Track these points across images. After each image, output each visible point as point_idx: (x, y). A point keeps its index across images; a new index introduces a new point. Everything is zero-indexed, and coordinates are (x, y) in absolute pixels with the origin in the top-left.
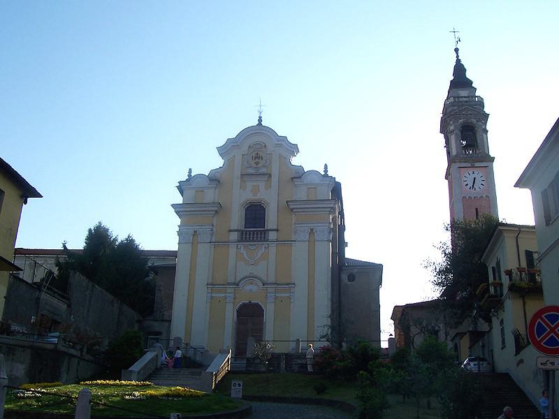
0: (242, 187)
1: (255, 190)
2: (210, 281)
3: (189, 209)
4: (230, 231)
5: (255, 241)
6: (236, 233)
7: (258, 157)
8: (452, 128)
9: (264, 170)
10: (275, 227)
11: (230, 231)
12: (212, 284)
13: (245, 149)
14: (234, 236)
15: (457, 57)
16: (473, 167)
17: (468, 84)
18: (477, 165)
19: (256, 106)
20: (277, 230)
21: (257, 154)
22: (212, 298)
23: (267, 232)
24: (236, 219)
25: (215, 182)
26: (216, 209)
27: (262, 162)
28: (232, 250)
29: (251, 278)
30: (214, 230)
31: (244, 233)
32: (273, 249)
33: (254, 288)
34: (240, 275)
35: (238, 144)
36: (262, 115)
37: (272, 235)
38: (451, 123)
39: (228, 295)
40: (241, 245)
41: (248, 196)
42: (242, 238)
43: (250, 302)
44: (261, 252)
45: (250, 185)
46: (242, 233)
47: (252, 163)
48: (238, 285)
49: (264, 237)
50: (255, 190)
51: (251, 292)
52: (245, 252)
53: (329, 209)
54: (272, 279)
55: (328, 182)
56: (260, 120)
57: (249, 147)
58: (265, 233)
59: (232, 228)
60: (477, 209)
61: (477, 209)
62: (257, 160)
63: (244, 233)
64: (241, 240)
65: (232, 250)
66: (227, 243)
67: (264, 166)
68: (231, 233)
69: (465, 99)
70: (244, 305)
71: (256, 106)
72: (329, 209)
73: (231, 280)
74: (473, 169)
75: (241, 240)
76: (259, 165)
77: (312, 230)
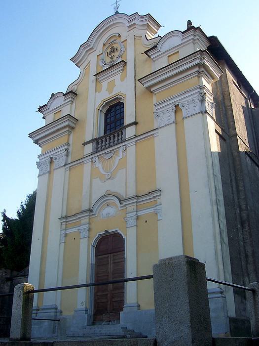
1: (111, 86)
2: (64, 215)
4: (84, 144)
10: (133, 120)
12: (66, 217)
13: (100, 49)
22: (66, 235)
27: (116, 54)
32: (131, 149)
33: (111, 210)
39: (81, 227)
45: (105, 84)
46: (98, 143)
51: (109, 218)
53: (197, 69)
54: (131, 192)
55: (192, 37)
57: (104, 45)
64: (96, 150)
65: (87, 167)
66: (79, 161)
73: (86, 206)
75: (96, 150)
76: (115, 59)
77: (177, 106)
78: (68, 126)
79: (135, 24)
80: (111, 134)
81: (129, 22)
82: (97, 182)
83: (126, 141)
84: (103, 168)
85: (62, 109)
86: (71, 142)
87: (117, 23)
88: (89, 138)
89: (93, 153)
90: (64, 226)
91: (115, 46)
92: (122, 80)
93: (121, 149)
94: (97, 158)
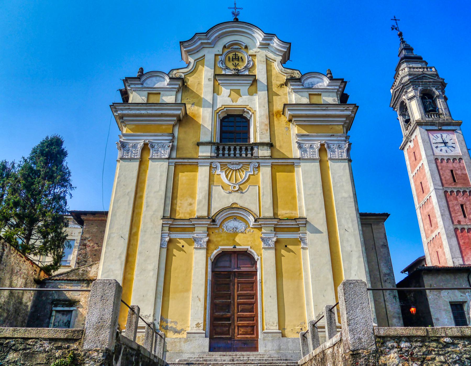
3: (138, 112)
4: (199, 144)
5: (237, 158)
6: (209, 148)
8: (411, 95)
9: (247, 73)
10: (267, 140)
13: (219, 48)
14: (205, 152)
15: (402, 39)
16: (440, 130)
17: (418, 59)
18: (444, 128)
19: (229, 8)
20: (271, 145)
21: (235, 54)
23: (255, 149)
25: (180, 83)
26: (178, 112)
30: (175, 143)
34: (216, 207)
36: (237, 17)
38: (410, 90)
40: (217, 162)
41: (226, 99)
42: (218, 155)
43: (235, 247)
46: (218, 149)
48: (214, 221)
49: (252, 154)
52: (223, 175)
53: (344, 119)
55: (338, 87)
57: (225, 47)
58: (252, 149)
59: (201, 140)
60: (452, 171)
61: (452, 171)
68: (201, 148)
69: (421, 70)
70: (223, 254)
71: (229, 8)
72: (344, 119)
74: (441, 132)
78: (178, 116)
80: (238, 145)
84: (227, 176)
85: (162, 93)
86: (176, 134)
87: (244, 32)
88: (205, 138)
89: (211, 157)
91: (240, 55)
93: (252, 165)
94: (219, 165)
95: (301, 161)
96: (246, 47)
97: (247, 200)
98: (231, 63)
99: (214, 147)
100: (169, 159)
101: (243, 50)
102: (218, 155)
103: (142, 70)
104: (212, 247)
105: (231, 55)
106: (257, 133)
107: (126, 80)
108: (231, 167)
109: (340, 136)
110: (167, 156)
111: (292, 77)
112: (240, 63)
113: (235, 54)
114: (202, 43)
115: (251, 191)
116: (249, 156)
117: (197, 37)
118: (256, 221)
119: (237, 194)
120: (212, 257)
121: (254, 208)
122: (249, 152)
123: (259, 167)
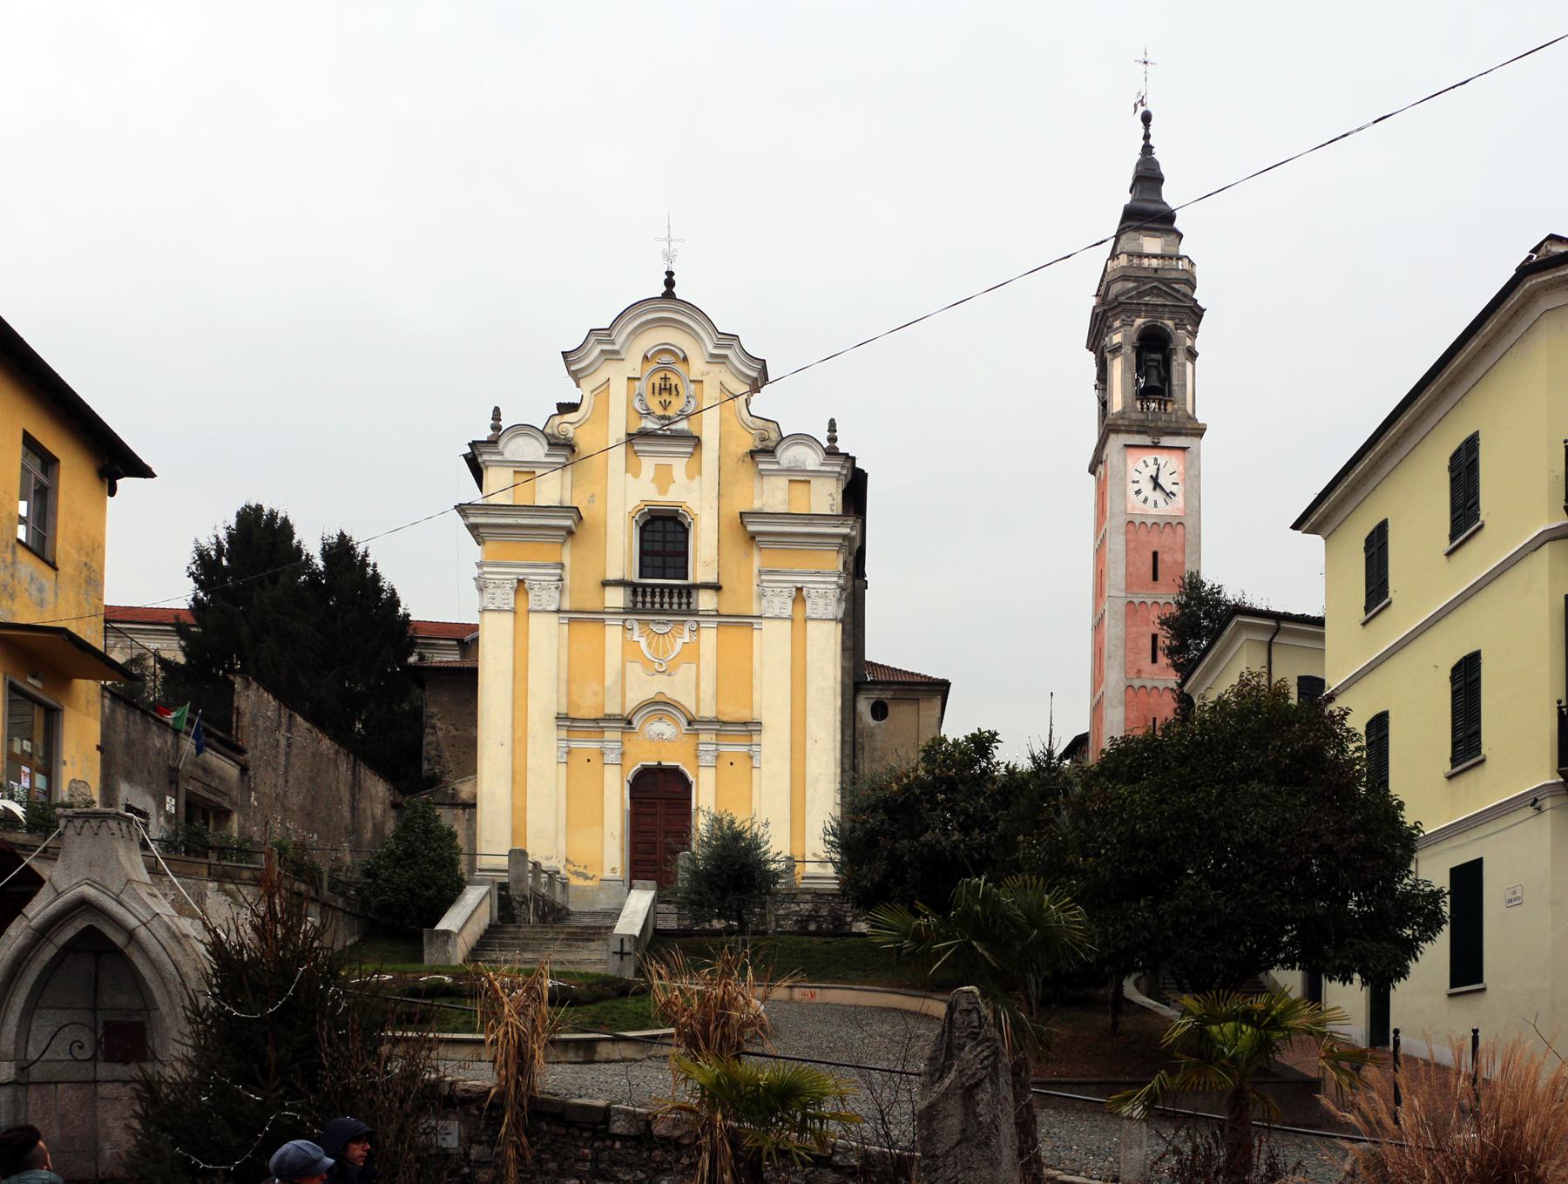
0: (632, 469)
1: (663, 478)
2: (563, 710)
4: (606, 584)
7: (666, 388)
9: (683, 425)
10: (712, 579)
11: (606, 584)
13: (633, 363)
20: (717, 588)
21: (665, 378)
23: (694, 593)
24: (620, 552)
27: (677, 405)
28: (613, 634)
29: (660, 706)
31: (640, 590)
34: (635, 697)
35: (616, 348)
37: (705, 601)
42: (635, 604)
44: (680, 642)
45: (648, 465)
46: (635, 593)
47: (654, 404)
48: (630, 722)
49: (688, 604)
50: (663, 478)
51: (659, 743)
52: (643, 642)
54: (708, 712)
56: (670, 283)
57: (645, 357)
58: (689, 595)
62: (665, 396)
63: (640, 590)
65: (613, 634)
67: (685, 415)
68: (608, 589)
73: (613, 708)
79: (726, 356)
81: (717, 346)
82: (635, 670)
83: (695, 613)
84: (649, 645)
89: (626, 611)
90: (563, 734)
91: (674, 380)
92: (690, 477)
95: (764, 622)
96: (685, 359)
97: (678, 688)
98: (658, 399)
99: (629, 591)
100: (558, 611)
101: (680, 367)
102: (635, 604)
103: (497, 414)
104: (628, 762)
105: (657, 379)
106: (702, 566)
107: (473, 445)
108: (654, 628)
109: (830, 575)
110: (554, 607)
111: (763, 440)
112: (673, 398)
113: (665, 378)
114: (603, 351)
115: (686, 672)
116: (684, 607)
117: (593, 339)
118: (689, 724)
119: (662, 677)
120: (630, 778)
121: (689, 702)
122: (684, 600)
123: (699, 628)
